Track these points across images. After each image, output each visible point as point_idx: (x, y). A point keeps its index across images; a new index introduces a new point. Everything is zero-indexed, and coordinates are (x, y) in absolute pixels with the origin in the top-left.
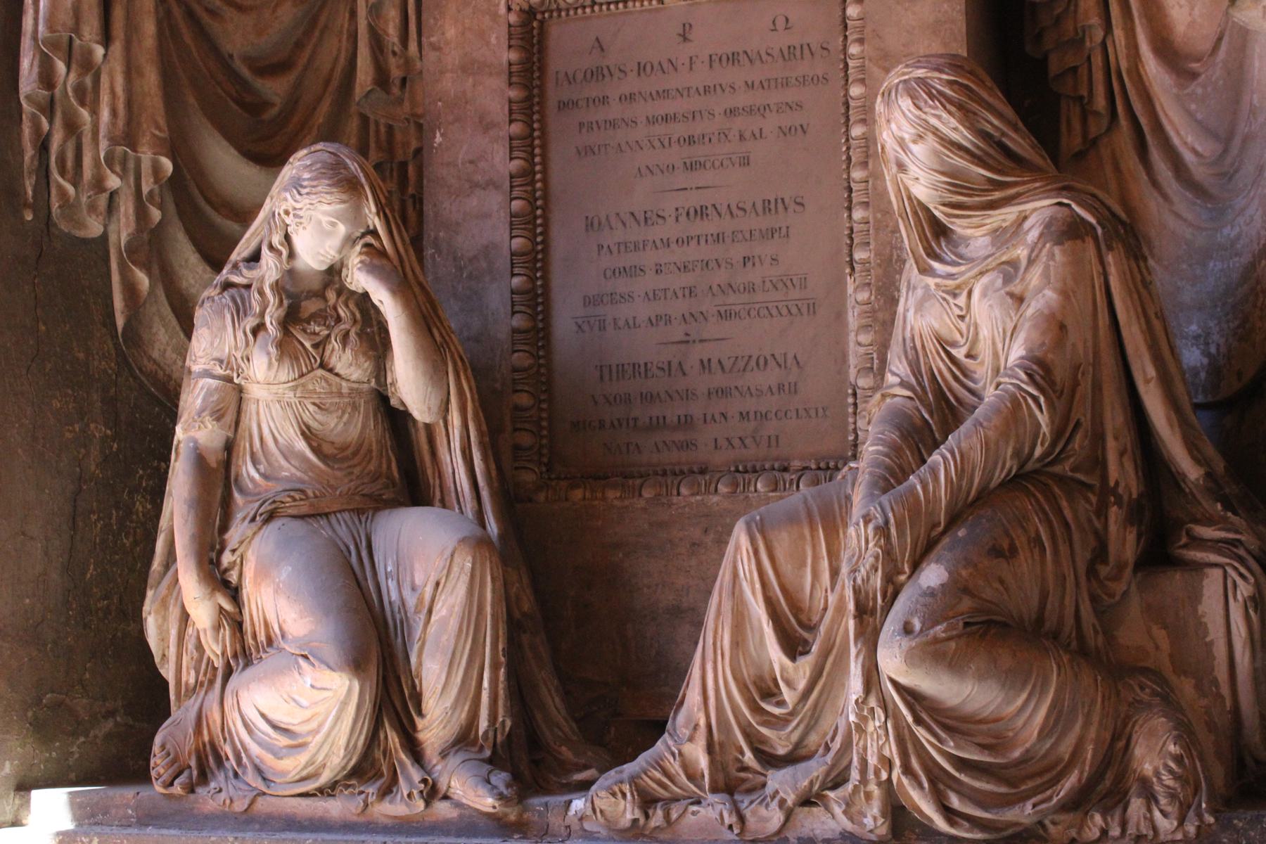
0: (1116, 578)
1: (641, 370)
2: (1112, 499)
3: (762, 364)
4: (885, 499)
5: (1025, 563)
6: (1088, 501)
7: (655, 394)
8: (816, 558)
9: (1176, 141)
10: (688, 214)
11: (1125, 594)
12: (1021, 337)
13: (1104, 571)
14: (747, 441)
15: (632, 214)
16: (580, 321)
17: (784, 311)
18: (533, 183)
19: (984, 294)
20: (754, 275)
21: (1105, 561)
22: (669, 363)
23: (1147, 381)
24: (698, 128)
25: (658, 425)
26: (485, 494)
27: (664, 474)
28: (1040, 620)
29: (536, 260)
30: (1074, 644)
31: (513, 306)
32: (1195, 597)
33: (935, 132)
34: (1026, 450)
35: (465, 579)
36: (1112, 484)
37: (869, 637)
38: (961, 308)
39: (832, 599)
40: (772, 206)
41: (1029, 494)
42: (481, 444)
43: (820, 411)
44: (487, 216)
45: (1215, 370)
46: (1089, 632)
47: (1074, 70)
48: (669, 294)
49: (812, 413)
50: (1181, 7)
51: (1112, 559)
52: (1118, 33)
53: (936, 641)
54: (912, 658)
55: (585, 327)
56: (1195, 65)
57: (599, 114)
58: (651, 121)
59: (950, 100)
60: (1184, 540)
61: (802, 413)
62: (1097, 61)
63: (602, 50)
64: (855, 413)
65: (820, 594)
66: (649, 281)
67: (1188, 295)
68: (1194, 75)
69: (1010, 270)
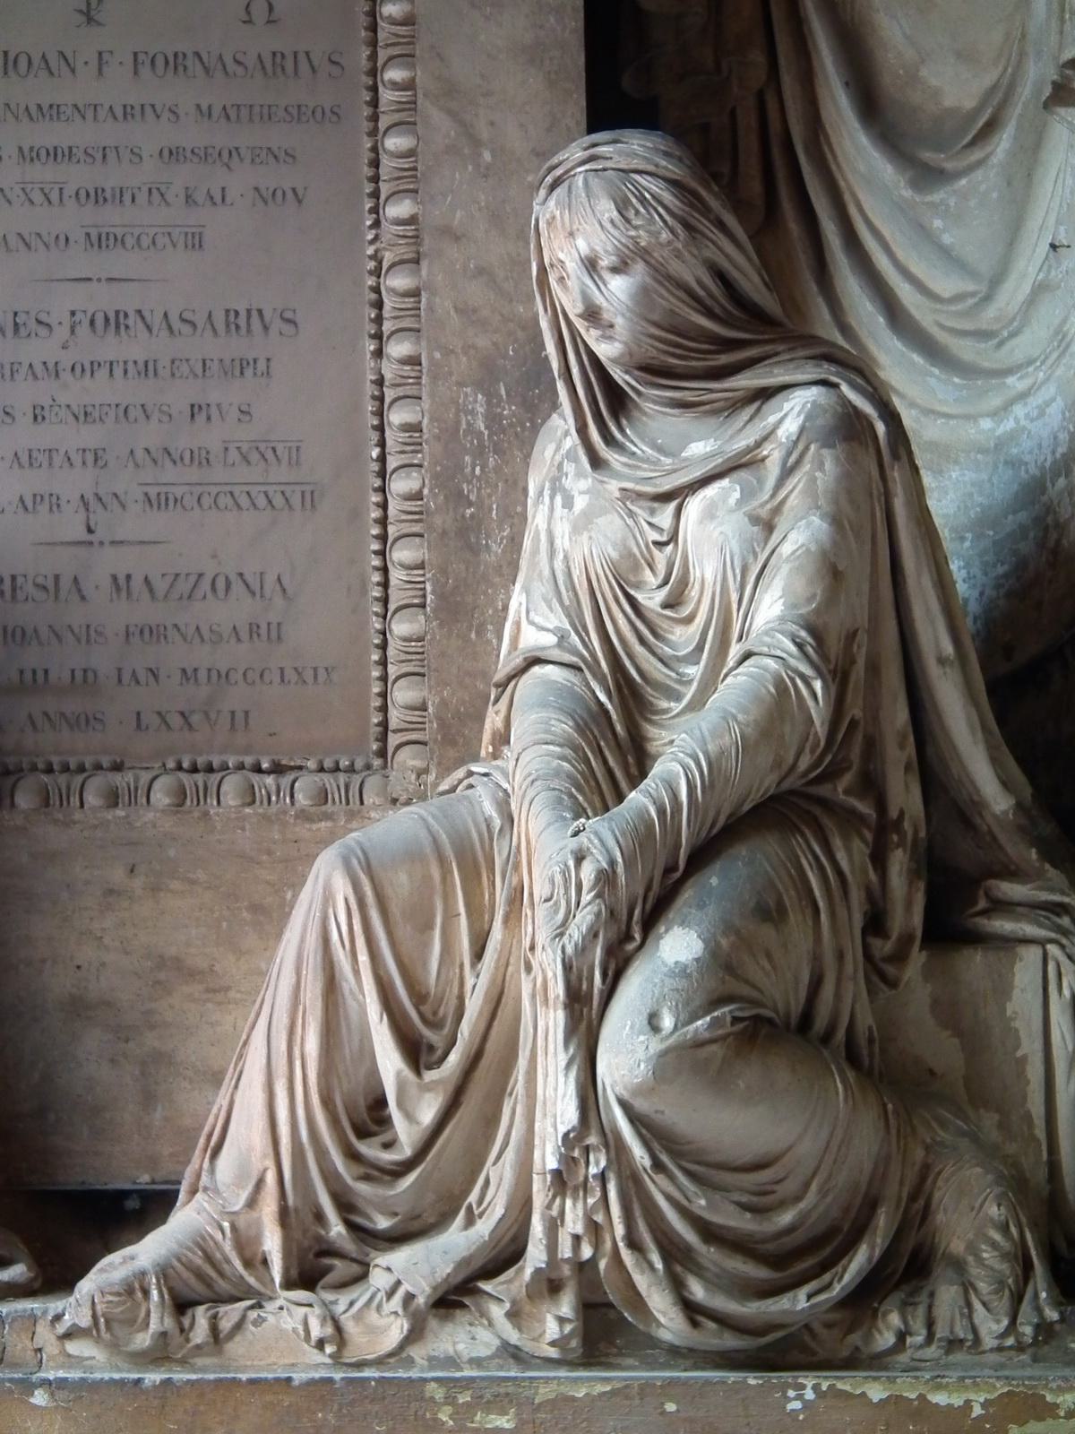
2: (895, 838)
3: (221, 587)
7: (29, 632)
8: (450, 916)
10: (92, 322)
14: (195, 719)
17: (261, 502)
20: (210, 437)
22: (57, 578)
24: (111, 177)
32: (1003, 990)
34: (790, 760)
36: (894, 814)
40: (242, 321)
43: (322, 675)
48: (58, 459)
49: (309, 675)
60: (982, 904)
64: (384, 678)
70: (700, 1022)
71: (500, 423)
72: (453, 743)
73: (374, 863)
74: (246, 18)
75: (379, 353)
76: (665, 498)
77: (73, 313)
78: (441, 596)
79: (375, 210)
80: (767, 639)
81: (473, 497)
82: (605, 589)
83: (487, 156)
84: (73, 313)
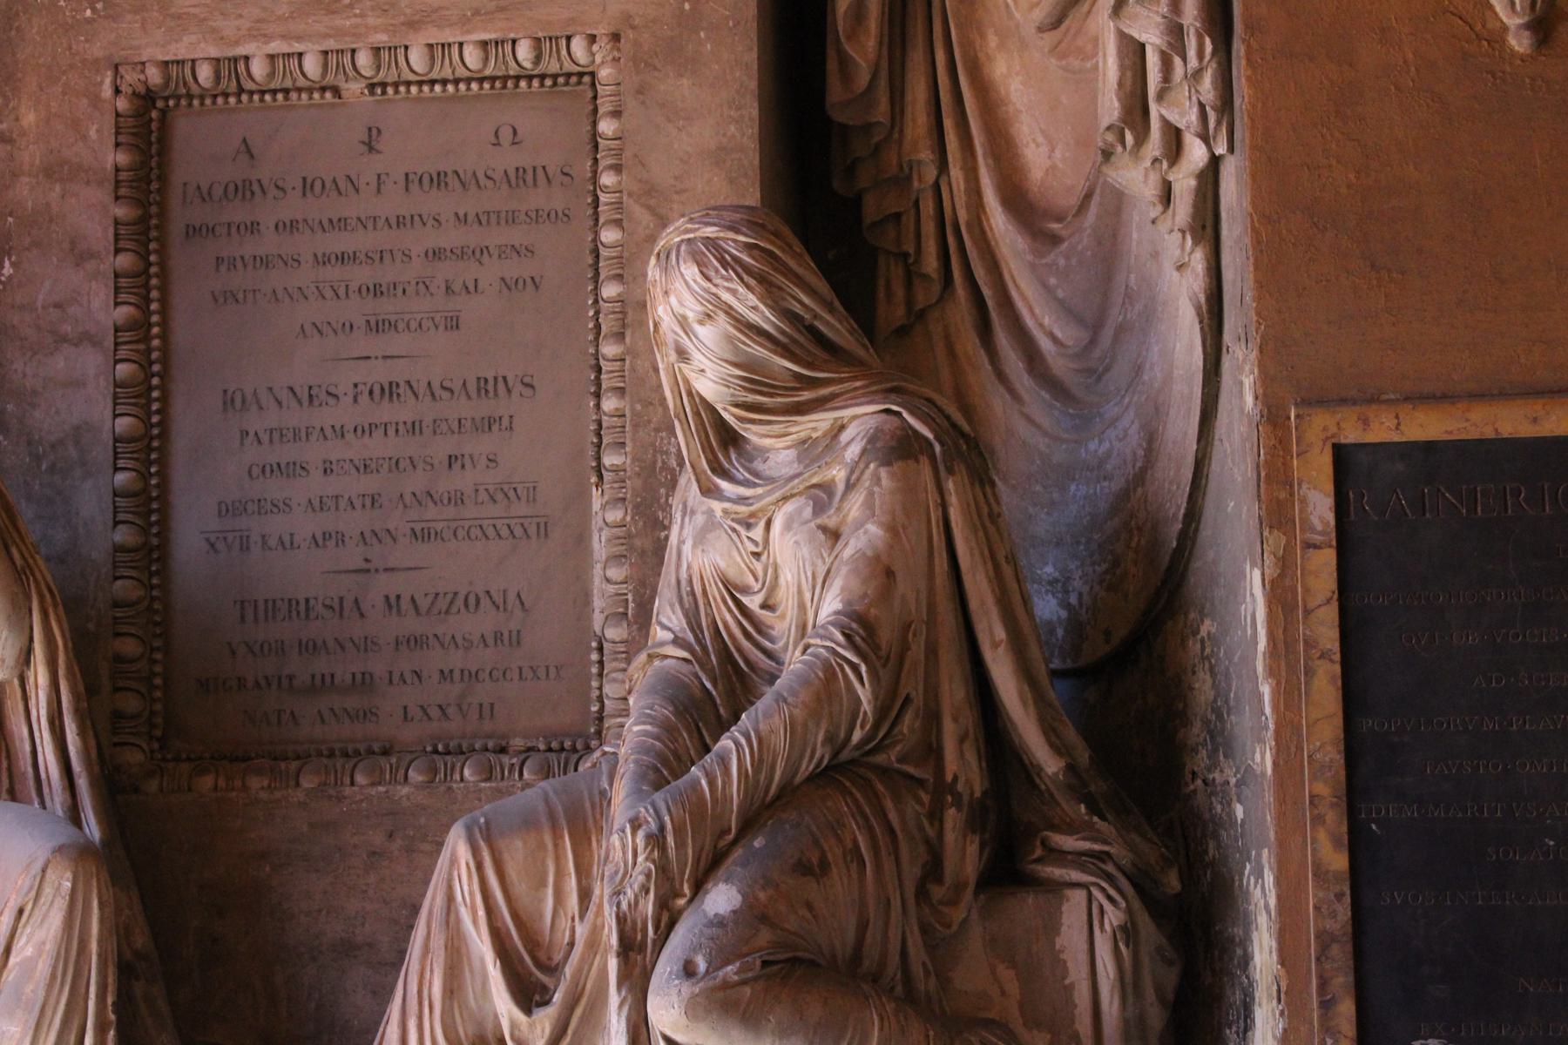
0: (953, 902)
1: (302, 609)
2: (949, 798)
3: (472, 603)
4: (659, 797)
5: (840, 884)
6: (919, 801)
7: (319, 643)
9: (1029, 322)
10: (371, 392)
11: (965, 921)
12: (837, 584)
13: (937, 892)
14: (451, 711)
15: (291, 389)
16: (213, 538)
17: (505, 532)
18: (147, 338)
19: (788, 526)
20: (463, 480)
21: (939, 880)
22: (341, 599)
23: (995, 645)
24: (386, 274)
25: (321, 685)
26: (82, 783)
27: (331, 755)
28: (857, 957)
29: (149, 448)
30: (899, 989)
31: (115, 513)
32: (1052, 927)
33: (729, 311)
34: (842, 735)
35: (61, 905)
36: (949, 778)
37: (637, 981)
38: (756, 543)
39: (586, 930)
40: (490, 387)
41: (845, 792)
42: (78, 713)
43: (552, 671)
44: (79, 384)
45: (1076, 627)
46: (917, 970)
47: (897, 216)
48: (343, 504)
49: (542, 673)
50: (1038, 146)
51: (948, 880)
52: (956, 172)
53: (726, 985)
54: (694, 1009)
55: (220, 546)
56: (1055, 226)
57: (250, 247)
58: (322, 260)
59: (748, 270)
60: (1038, 852)
61: (527, 673)
62: (928, 208)
63: (252, 157)
64: (600, 675)
65: (564, 924)
66: (315, 485)
67: (1043, 525)
68: (1055, 240)
69: (822, 497)
70: (730, 968)
74: (494, 140)
77: (356, 386)
84: (356, 386)
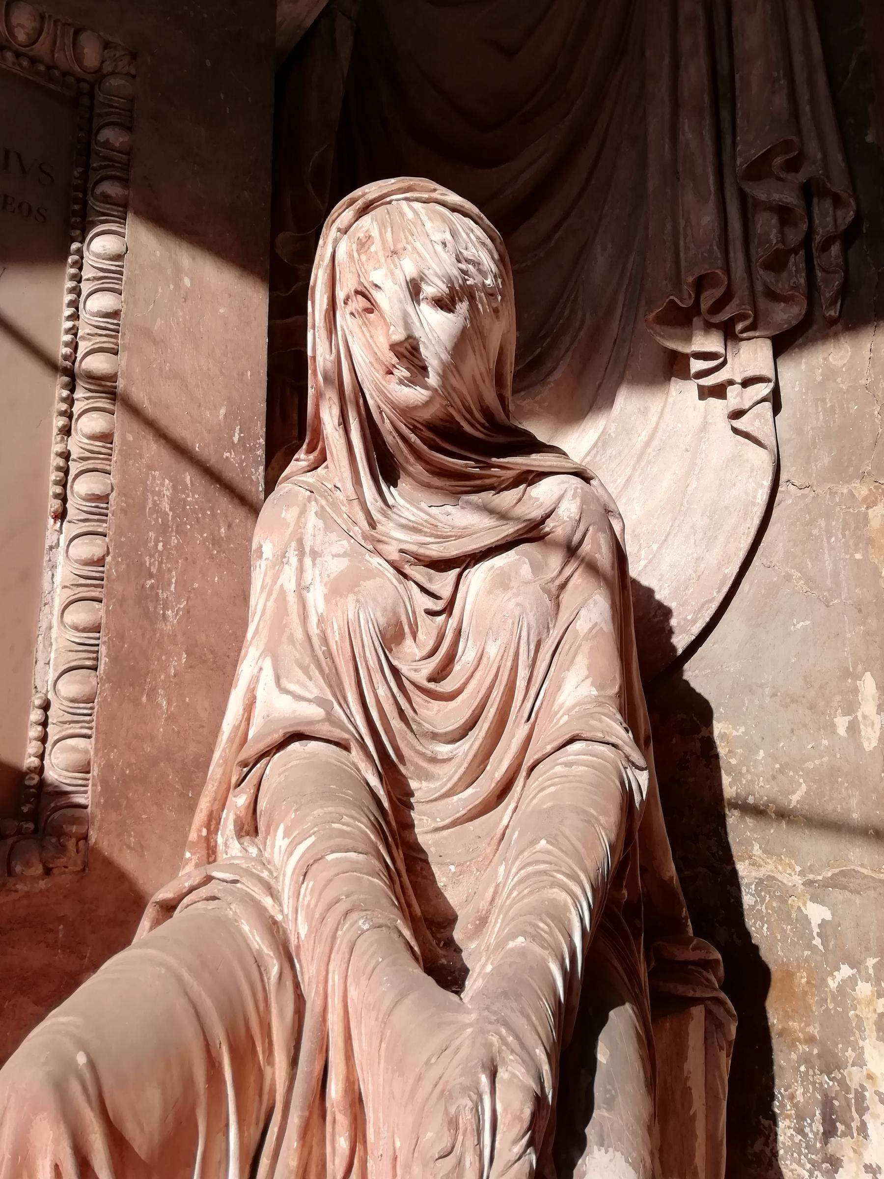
71: (184, 508)
72: (117, 806)
73: (102, 1068)
75: (66, 431)
76: (440, 565)
78: (114, 660)
79: (74, 304)
80: (593, 722)
81: (154, 570)
82: (370, 654)
83: (187, 282)
